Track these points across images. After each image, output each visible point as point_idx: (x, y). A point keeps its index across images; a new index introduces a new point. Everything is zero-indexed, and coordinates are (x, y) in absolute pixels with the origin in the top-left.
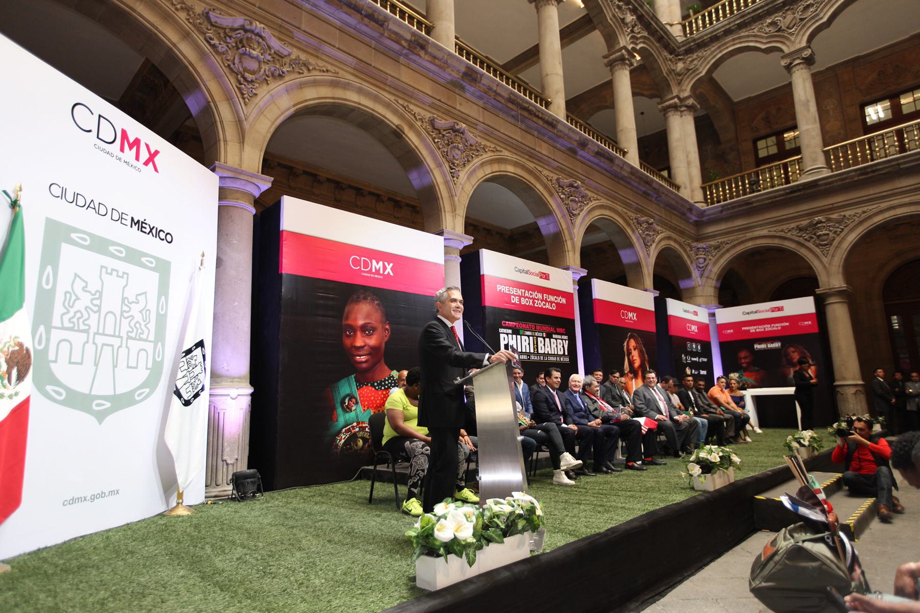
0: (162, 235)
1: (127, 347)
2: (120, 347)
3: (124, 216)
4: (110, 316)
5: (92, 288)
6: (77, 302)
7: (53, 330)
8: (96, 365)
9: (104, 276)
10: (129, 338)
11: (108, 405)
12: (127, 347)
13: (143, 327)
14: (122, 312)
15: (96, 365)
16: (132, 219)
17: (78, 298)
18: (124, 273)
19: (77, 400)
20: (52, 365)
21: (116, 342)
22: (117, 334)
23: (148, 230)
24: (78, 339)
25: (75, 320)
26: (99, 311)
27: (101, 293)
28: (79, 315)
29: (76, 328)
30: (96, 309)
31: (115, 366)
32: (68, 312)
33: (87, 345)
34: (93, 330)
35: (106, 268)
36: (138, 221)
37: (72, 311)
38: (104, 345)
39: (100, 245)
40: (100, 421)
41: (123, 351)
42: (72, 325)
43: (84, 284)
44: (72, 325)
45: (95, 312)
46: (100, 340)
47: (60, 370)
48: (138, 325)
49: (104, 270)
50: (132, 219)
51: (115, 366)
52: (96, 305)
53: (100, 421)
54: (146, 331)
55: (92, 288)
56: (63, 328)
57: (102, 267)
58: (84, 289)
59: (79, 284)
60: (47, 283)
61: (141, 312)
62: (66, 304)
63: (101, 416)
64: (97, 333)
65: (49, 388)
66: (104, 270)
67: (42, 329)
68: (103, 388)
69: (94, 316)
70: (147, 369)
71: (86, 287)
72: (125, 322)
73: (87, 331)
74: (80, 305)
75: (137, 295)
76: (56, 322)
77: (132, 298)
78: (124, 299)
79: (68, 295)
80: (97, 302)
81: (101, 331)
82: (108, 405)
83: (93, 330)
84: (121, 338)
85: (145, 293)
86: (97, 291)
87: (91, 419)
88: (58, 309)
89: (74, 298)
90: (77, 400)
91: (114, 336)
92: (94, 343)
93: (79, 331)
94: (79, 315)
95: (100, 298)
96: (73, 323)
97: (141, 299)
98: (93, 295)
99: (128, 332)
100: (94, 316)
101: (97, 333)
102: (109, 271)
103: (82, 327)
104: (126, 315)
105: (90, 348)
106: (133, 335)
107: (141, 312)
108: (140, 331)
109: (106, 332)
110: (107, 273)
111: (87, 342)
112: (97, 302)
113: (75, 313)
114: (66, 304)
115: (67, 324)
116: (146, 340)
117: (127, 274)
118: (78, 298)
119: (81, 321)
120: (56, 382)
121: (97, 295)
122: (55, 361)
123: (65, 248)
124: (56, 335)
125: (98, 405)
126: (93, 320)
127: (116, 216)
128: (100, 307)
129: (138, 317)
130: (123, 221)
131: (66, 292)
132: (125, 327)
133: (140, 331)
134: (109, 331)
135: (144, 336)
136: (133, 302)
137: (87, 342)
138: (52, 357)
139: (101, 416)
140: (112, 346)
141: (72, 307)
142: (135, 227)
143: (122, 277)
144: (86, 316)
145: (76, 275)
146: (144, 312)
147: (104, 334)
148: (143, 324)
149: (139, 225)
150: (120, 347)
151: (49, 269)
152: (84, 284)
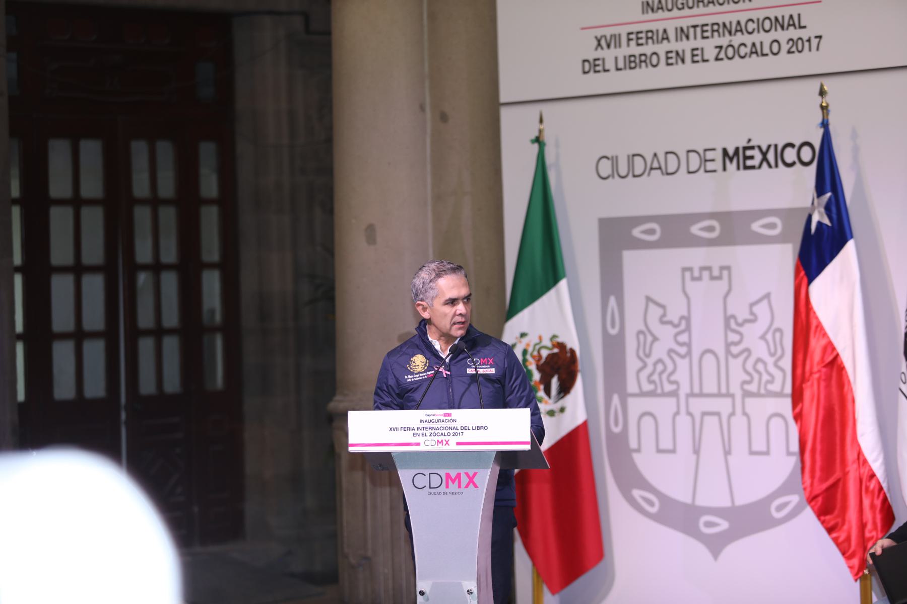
0: (790, 155)
1: (745, 414)
2: (733, 414)
3: (709, 155)
4: (709, 359)
5: (674, 315)
6: (656, 345)
7: (631, 401)
8: (697, 451)
9: (690, 285)
10: (747, 394)
11: (724, 525)
12: (745, 414)
13: (772, 369)
14: (728, 345)
15: (697, 451)
16: (725, 152)
17: (655, 339)
18: (722, 268)
19: (681, 516)
20: (635, 456)
21: (723, 405)
22: (724, 390)
23: (758, 157)
24: (663, 407)
25: (655, 377)
26: (689, 353)
27: (687, 319)
28: (660, 367)
29: (659, 391)
30: (683, 350)
31: (727, 453)
32: (645, 366)
33: (678, 418)
34: (684, 389)
35: (690, 269)
36: (737, 149)
37: (650, 361)
38: (704, 414)
39: (675, 231)
40: (716, 554)
41: (739, 422)
42: (651, 387)
43: (660, 311)
44: (651, 387)
45: (682, 357)
46: (698, 405)
47: (647, 463)
48: (760, 367)
49: (688, 274)
50: (725, 152)
51: (727, 453)
52: (681, 344)
53: (716, 554)
54: (778, 375)
55: (674, 315)
56: (643, 394)
57: (685, 270)
58: (663, 321)
59: (655, 312)
60: (613, 326)
61: (763, 337)
62: (641, 354)
63: (715, 545)
64: (692, 395)
65: (637, 493)
66: (688, 274)
67: (616, 400)
68: (713, 495)
69: (683, 364)
70: (789, 453)
71: (664, 315)
72: (735, 365)
73: (674, 394)
74: (659, 351)
75: (752, 305)
76: (632, 387)
77: (742, 314)
78: (728, 319)
79: (641, 337)
80: (683, 338)
81: (696, 390)
82: (724, 525)
83: (684, 389)
84: (732, 396)
85: (767, 296)
86: (682, 318)
87: (700, 550)
88: (632, 364)
89: (649, 338)
90: (681, 516)
91: (719, 395)
92: (689, 414)
93: (664, 395)
94: (660, 367)
95: (688, 329)
96: (653, 382)
97: (762, 310)
98: (676, 326)
99: (745, 382)
100: (683, 364)
101: (692, 395)
102: (696, 274)
103: (668, 388)
104: (735, 350)
105: (684, 421)
106: (753, 387)
107: (763, 337)
108: (765, 377)
109: (706, 390)
110: (694, 279)
111: (677, 413)
112: (683, 338)
113: (655, 364)
114: (641, 354)
115: (647, 387)
116: (779, 395)
117: (728, 268)
118: (655, 339)
119: (664, 376)
120: (646, 485)
121: (683, 326)
122: (638, 450)
123: (629, 257)
124: (636, 406)
125: (709, 524)
126: (682, 376)
127: (695, 161)
128: (688, 345)
129: (760, 350)
130: (710, 166)
131: (640, 332)
132: (737, 375)
133: (765, 377)
134: (710, 386)
135: (775, 387)
136: (747, 321)
137: (677, 413)
138: (633, 444)
139: (715, 545)
140: (718, 414)
141: (648, 356)
142: (732, 167)
143: (719, 278)
144: (670, 367)
145: (649, 299)
146: (769, 337)
147: (701, 395)
148: (770, 361)
149: (738, 157)
150: (733, 414)
151: (612, 301)
152: (660, 311)
